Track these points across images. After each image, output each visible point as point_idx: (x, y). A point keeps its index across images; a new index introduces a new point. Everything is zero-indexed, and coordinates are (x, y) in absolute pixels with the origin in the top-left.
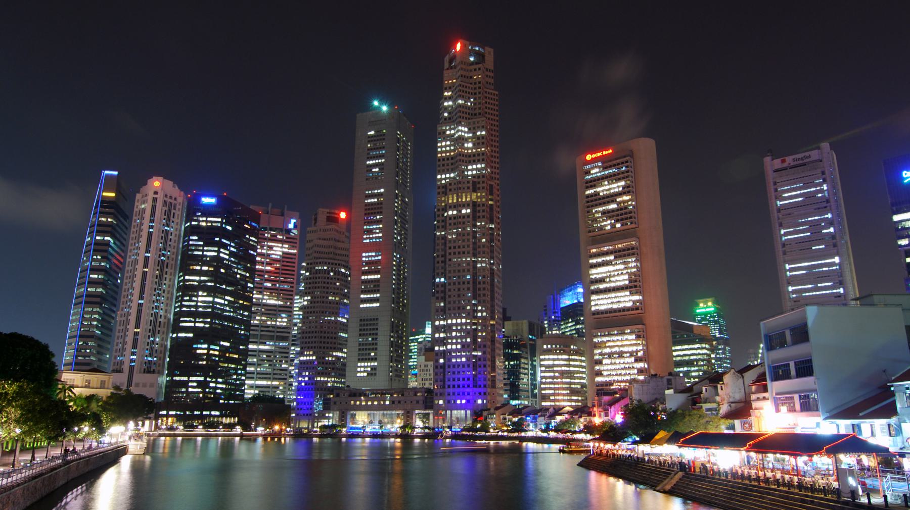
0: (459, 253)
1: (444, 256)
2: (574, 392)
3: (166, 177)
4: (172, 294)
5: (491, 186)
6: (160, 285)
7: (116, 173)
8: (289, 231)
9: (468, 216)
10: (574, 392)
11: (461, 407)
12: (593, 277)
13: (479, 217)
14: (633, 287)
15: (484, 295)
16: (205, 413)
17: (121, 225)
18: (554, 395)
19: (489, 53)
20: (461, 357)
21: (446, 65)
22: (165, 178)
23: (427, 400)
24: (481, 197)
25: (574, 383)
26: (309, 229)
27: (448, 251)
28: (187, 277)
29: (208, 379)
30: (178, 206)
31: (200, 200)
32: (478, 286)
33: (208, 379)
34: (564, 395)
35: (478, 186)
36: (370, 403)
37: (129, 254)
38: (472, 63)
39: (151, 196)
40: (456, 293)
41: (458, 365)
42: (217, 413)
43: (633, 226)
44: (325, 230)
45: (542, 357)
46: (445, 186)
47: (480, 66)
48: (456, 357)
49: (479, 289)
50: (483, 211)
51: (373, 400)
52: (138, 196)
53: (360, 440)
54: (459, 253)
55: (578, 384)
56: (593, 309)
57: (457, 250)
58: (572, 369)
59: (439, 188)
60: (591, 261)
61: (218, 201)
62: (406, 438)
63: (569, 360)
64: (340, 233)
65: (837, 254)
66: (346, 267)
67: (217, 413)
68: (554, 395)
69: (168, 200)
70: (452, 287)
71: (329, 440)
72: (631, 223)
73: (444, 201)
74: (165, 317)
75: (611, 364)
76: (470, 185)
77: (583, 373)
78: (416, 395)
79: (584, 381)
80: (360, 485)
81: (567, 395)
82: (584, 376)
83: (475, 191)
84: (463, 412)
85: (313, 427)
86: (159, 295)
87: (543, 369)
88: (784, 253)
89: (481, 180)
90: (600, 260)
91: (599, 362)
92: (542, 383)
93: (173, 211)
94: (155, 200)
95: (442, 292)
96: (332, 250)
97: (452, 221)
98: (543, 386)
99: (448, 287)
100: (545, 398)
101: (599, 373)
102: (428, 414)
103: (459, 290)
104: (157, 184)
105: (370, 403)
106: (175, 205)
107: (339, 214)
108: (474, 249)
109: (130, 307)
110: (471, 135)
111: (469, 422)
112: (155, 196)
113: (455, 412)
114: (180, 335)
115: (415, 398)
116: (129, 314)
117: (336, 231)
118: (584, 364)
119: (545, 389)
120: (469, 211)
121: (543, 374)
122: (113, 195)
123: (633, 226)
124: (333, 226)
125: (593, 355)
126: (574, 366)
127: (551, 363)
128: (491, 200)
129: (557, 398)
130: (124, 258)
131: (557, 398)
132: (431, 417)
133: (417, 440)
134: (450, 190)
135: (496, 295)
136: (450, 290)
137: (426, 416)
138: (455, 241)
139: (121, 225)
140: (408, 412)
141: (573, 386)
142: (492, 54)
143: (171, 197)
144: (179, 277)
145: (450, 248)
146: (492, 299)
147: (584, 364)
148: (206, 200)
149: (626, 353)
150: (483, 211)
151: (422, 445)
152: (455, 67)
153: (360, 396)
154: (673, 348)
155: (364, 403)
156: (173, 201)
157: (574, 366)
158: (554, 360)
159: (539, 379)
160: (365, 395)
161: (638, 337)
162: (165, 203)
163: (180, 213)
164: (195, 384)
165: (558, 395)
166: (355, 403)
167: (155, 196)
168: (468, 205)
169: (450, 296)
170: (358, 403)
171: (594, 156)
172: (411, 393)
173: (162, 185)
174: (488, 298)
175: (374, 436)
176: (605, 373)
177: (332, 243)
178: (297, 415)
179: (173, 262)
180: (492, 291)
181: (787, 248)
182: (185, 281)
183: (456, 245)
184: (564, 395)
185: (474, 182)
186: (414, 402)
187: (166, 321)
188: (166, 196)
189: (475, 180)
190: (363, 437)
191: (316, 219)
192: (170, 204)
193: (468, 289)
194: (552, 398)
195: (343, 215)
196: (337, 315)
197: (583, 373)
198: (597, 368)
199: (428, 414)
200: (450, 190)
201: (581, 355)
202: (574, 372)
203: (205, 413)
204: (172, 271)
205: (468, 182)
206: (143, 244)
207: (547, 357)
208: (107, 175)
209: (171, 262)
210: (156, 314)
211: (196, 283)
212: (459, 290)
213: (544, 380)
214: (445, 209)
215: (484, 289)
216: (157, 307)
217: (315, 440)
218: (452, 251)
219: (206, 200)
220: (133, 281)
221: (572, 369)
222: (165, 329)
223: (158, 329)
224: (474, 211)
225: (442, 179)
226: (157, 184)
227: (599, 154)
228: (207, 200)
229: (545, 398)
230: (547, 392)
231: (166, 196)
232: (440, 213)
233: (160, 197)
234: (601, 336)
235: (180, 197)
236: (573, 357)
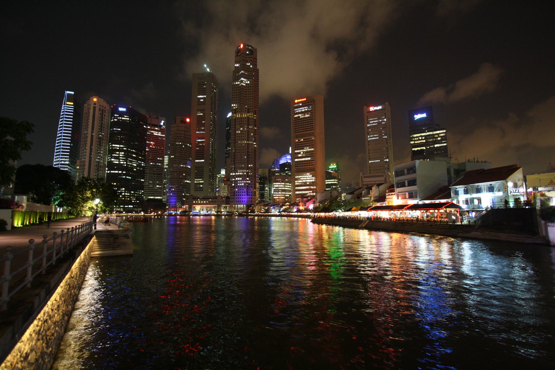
6: (100, 148)
7: (73, 93)
8: (161, 126)
20: (242, 183)
23: (228, 200)
24: (251, 115)
26: (172, 126)
31: (118, 109)
41: (241, 186)
48: (240, 183)
53: (198, 217)
61: (127, 110)
62: (218, 216)
66: (190, 144)
71: (184, 217)
74: (103, 163)
76: (246, 110)
80: (198, 236)
83: (248, 112)
94: (95, 108)
104: (95, 100)
108: (248, 138)
109: (85, 158)
111: (245, 210)
116: (85, 161)
124: (183, 125)
125: (295, 183)
133: (223, 217)
137: (226, 207)
148: (121, 109)
151: (225, 219)
152: (240, 55)
161: (313, 176)
162: (100, 110)
173: (98, 100)
175: (205, 215)
178: (169, 207)
182: (112, 147)
190: (200, 215)
191: (175, 121)
195: (188, 120)
196: (186, 164)
208: (68, 94)
209: (104, 138)
210: (99, 162)
217: (178, 217)
219: (121, 109)
220: (86, 146)
233: (97, 106)
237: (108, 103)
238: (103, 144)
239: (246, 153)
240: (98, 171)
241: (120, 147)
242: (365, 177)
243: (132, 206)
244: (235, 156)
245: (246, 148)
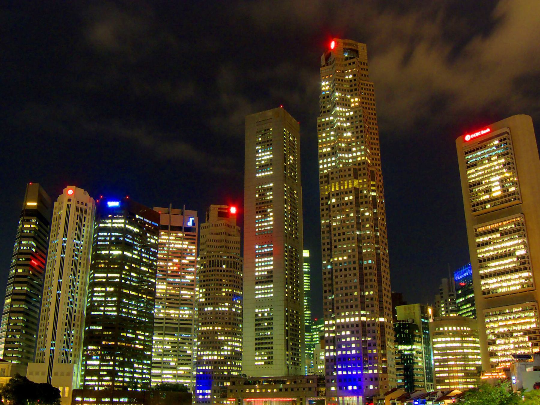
0: (344, 240)
1: (330, 243)
2: (468, 374)
3: (78, 186)
4: (85, 290)
5: (372, 172)
9: (351, 203)
10: (468, 374)
11: (353, 393)
12: (480, 256)
13: (362, 203)
14: (524, 264)
15: (371, 280)
16: (115, 400)
17: (42, 230)
18: (448, 378)
19: (363, 48)
21: (323, 62)
22: (77, 187)
24: (363, 183)
27: (333, 238)
28: (96, 275)
29: (117, 368)
31: (107, 205)
32: (365, 271)
33: (117, 368)
34: (458, 377)
35: (359, 172)
37: (49, 255)
38: (347, 59)
39: (66, 203)
40: (343, 279)
43: (517, 202)
44: (217, 225)
45: (434, 340)
46: (327, 176)
47: (354, 60)
49: (366, 274)
51: (266, 387)
52: (56, 204)
54: (344, 240)
55: (473, 365)
56: (483, 288)
58: (465, 351)
59: (322, 177)
60: (477, 240)
63: (462, 342)
64: (231, 227)
68: (448, 378)
69: (80, 205)
70: (339, 274)
72: (515, 199)
73: (327, 190)
75: (505, 343)
76: (352, 172)
77: (478, 354)
78: (308, 382)
79: (480, 363)
81: (462, 377)
82: (479, 357)
83: (356, 178)
84: (355, 398)
86: (73, 291)
87: (435, 352)
89: (362, 167)
90: (486, 238)
91: (493, 343)
92: (436, 366)
93: (84, 215)
94: (69, 206)
95: (329, 279)
96: (223, 244)
97: (336, 208)
98: (437, 369)
99: (335, 274)
100: (440, 381)
101: (493, 354)
103: (346, 276)
106: (86, 210)
107: (229, 209)
110: (348, 124)
112: (69, 203)
113: (347, 399)
114: (91, 327)
115: (307, 385)
116: (49, 309)
117: (227, 225)
118: (478, 345)
120: (351, 198)
121: (436, 357)
122: (35, 204)
123: (517, 202)
124: (223, 221)
126: (467, 348)
127: (443, 345)
129: (452, 381)
130: (46, 260)
131: (452, 381)
135: (383, 279)
136: (337, 277)
138: (339, 229)
139: (42, 230)
141: (468, 368)
142: (365, 48)
143: (82, 203)
144: (90, 275)
145: (335, 235)
146: (380, 282)
147: (478, 345)
149: (519, 331)
153: (255, 383)
155: (258, 391)
156: (84, 207)
157: (467, 348)
158: (446, 342)
159: (432, 362)
162: (77, 209)
163: (90, 217)
164: (105, 373)
165: (453, 378)
166: (250, 390)
167: (69, 203)
168: (351, 192)
169: (337, 283)
170: (253, 391)
171: (473, 136)
172: (304, 381)
174: (376, 284)
176: (499, 354)
177: (223, 237)
179: (85, 262)
180: (379, 275)
182: (94, 278)
183: (341, 231)
184: (458, 377)
185: (355, 170)
186: (307, 389)
187: (80, 315)
188: (78, 202)
189: (355, 167)
192: (82, 209)
193: (355, 275)
194: (446, 381)
195: (233, 210)
197: (478, 354)
198: (490, 348)
200: (332, 179)
201: (475, 337)
202: (468, 354)
203: (115, 400)
204: (84, 269)
205: (349, 170)
207: (439, 339)
211: (104, 280)
212: (346, 276)
213: (437, 364)
214: (328, 198)
215: (371, 274)
216: (72, 303)
218: (337, 238)
221: (465, 351)
222: (79, 323)
223: (73, 322)
224: (357, 198)
225: (324, 169)
226: (70, 192)
227: (477, 134)
228: (112, 204)
229: (440, 381)
230: (441, 375)
231: (78, 202)
232: (324, 201)
234: (493, 315)
235: (90, 203)
236: (466, 339)
237: (91, 195)
238: (80, 274)
239: (357, 271)
240: (69, 329)
241: (107, 278)
243: (126, 400)
244: (331, 279)
245: (356, 259)
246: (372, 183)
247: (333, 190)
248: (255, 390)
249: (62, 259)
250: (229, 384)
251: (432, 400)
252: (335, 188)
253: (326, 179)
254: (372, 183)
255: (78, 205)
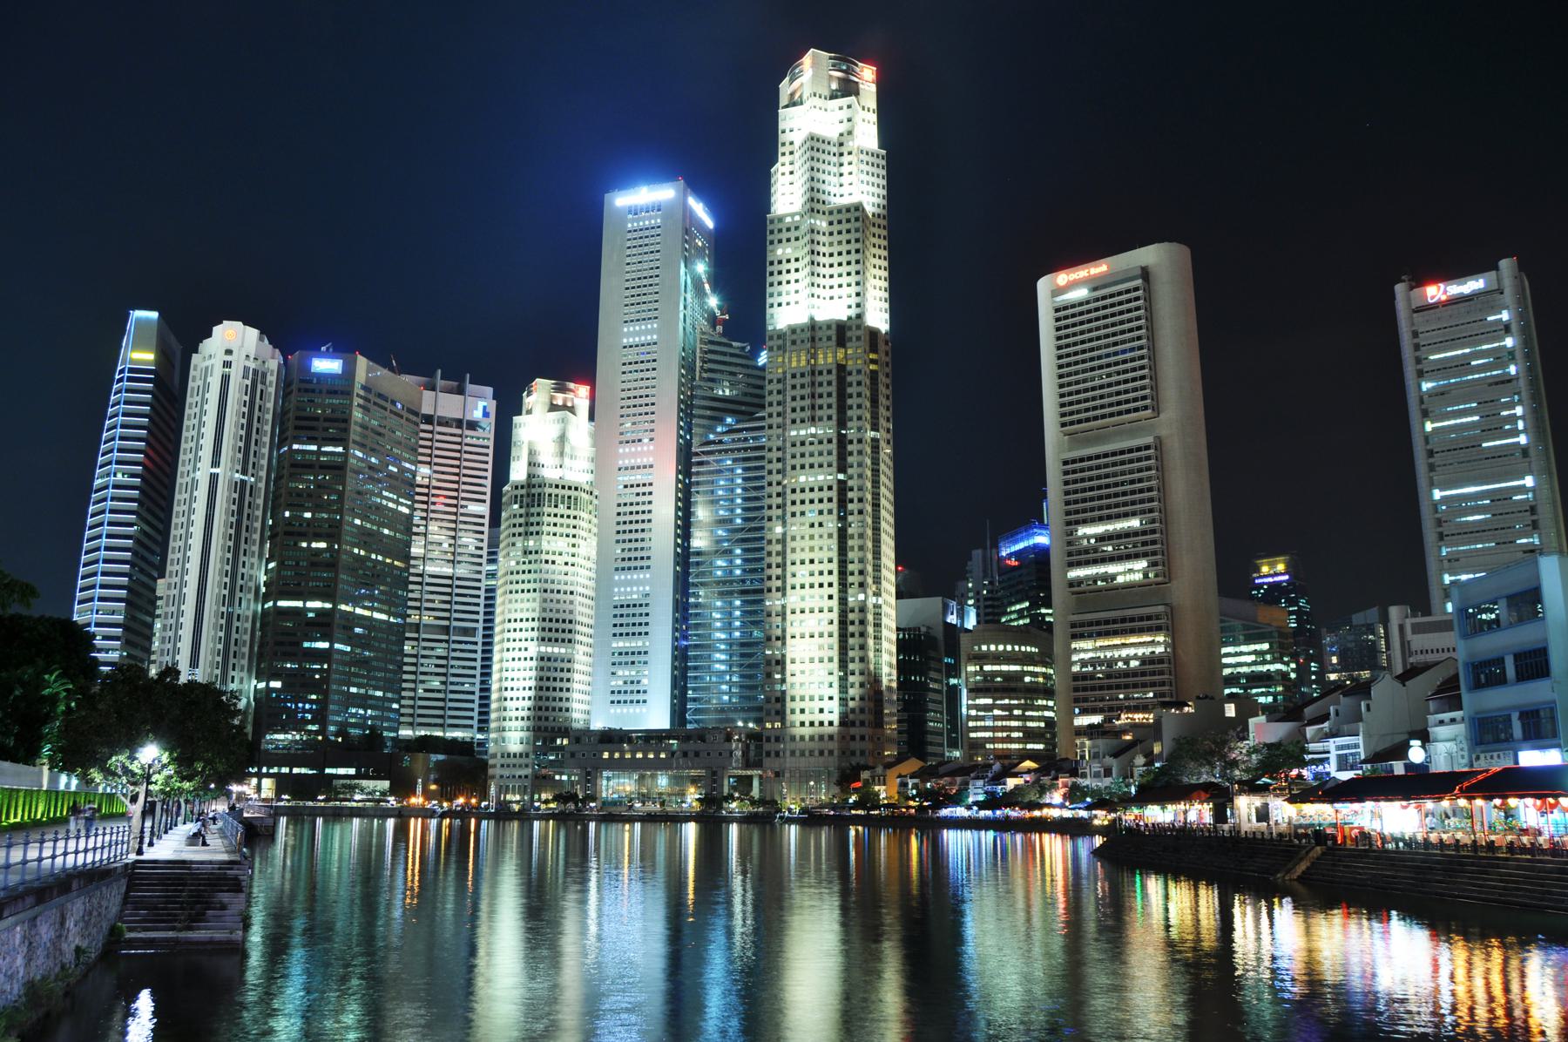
25: (1032, 719)
30: (269, 378)
36: (639, 755)
42: (352, 771)
50: (859, 383)
55: (1039, 719)
57: (807, 461)
65: (1530, 473)
67: (352, 771)
85: (532, 801)
88: (1432, 468)
92: (969, 718)
98: (971, 724)
102: (750, 778)
105: (639, 755)
112: (228, 358)
119: (976, 729)
128: (873, 361)
132: (756, 783)
134: (794, 342)
140: (714, 773)
150: (859, 383)
153: (621, 741)
154: (1224, 650)
155: (628, 756)
159: (964, 710)
160: (630, 741)
162: (246, 369)
167: (228, 358)
170: (617, 755)
181: (1437, 459)
199: (750, 778)
206: (206, 453)
208: (138, 321)
213: (973, 713)
230: (980, 735)
242: (1417, 629)
246: (872, 356)
247: (794, 364)
248: (622, 752)
249: (214, 479)
250: (565, 742)
251: (983, 778)
252: (799, 361)
253: (780, 342)
254: (872, 356)
255: (248, 364)
